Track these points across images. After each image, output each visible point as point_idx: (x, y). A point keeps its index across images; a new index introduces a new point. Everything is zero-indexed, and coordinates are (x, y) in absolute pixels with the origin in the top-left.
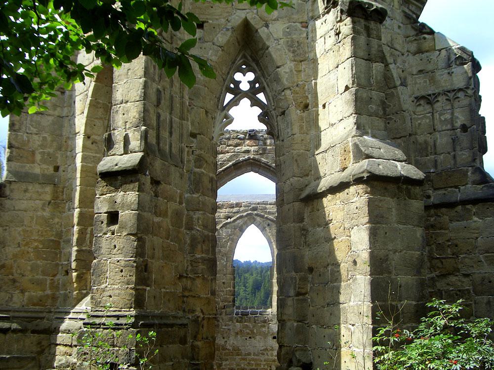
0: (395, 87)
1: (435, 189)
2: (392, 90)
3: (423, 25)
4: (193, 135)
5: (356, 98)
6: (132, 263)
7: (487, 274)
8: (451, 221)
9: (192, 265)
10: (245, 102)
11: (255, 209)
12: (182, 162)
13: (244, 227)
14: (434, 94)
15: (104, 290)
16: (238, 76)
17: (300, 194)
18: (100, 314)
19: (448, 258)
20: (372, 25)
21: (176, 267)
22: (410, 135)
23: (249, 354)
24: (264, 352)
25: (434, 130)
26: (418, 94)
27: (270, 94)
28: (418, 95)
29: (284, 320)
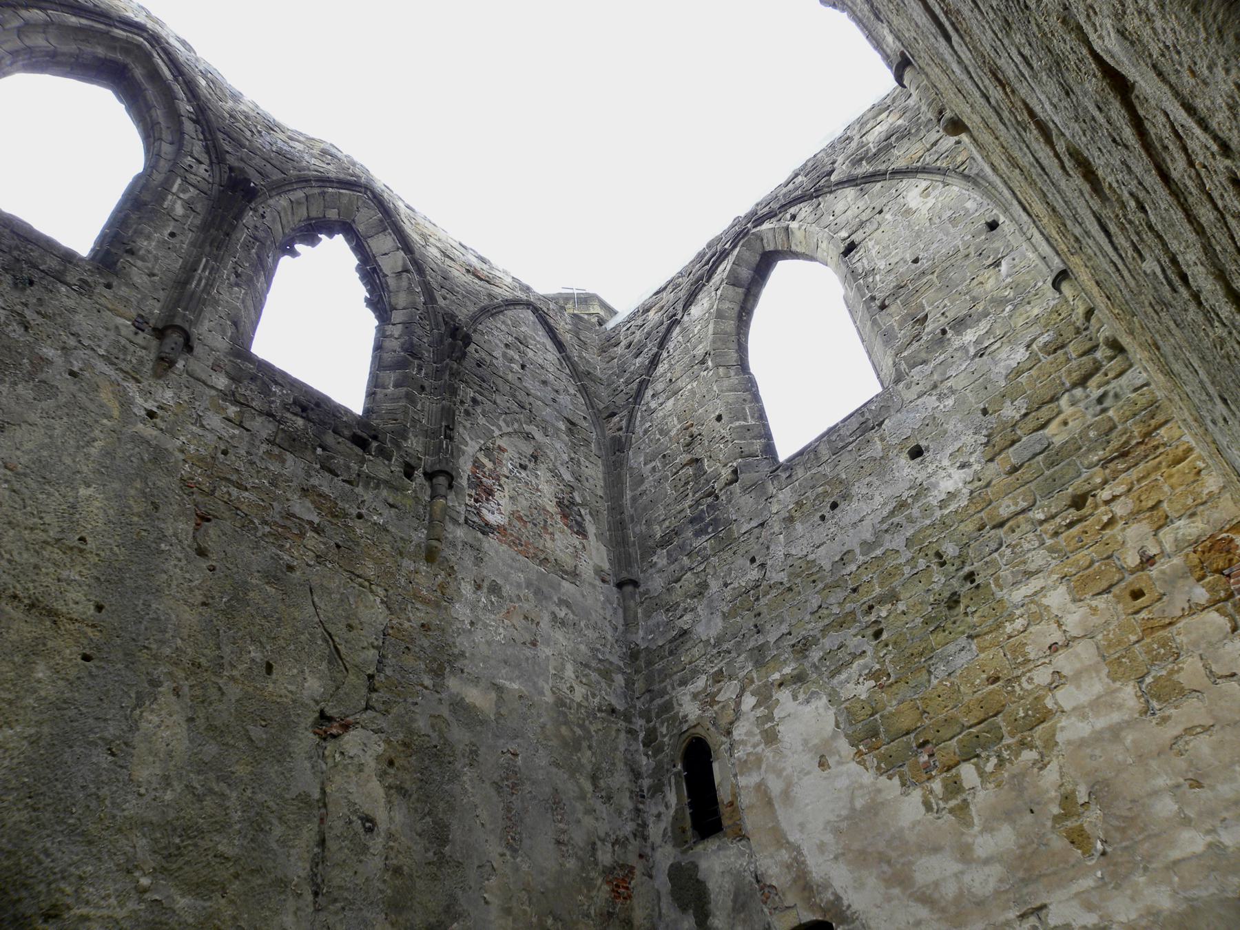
24: (896, 520)
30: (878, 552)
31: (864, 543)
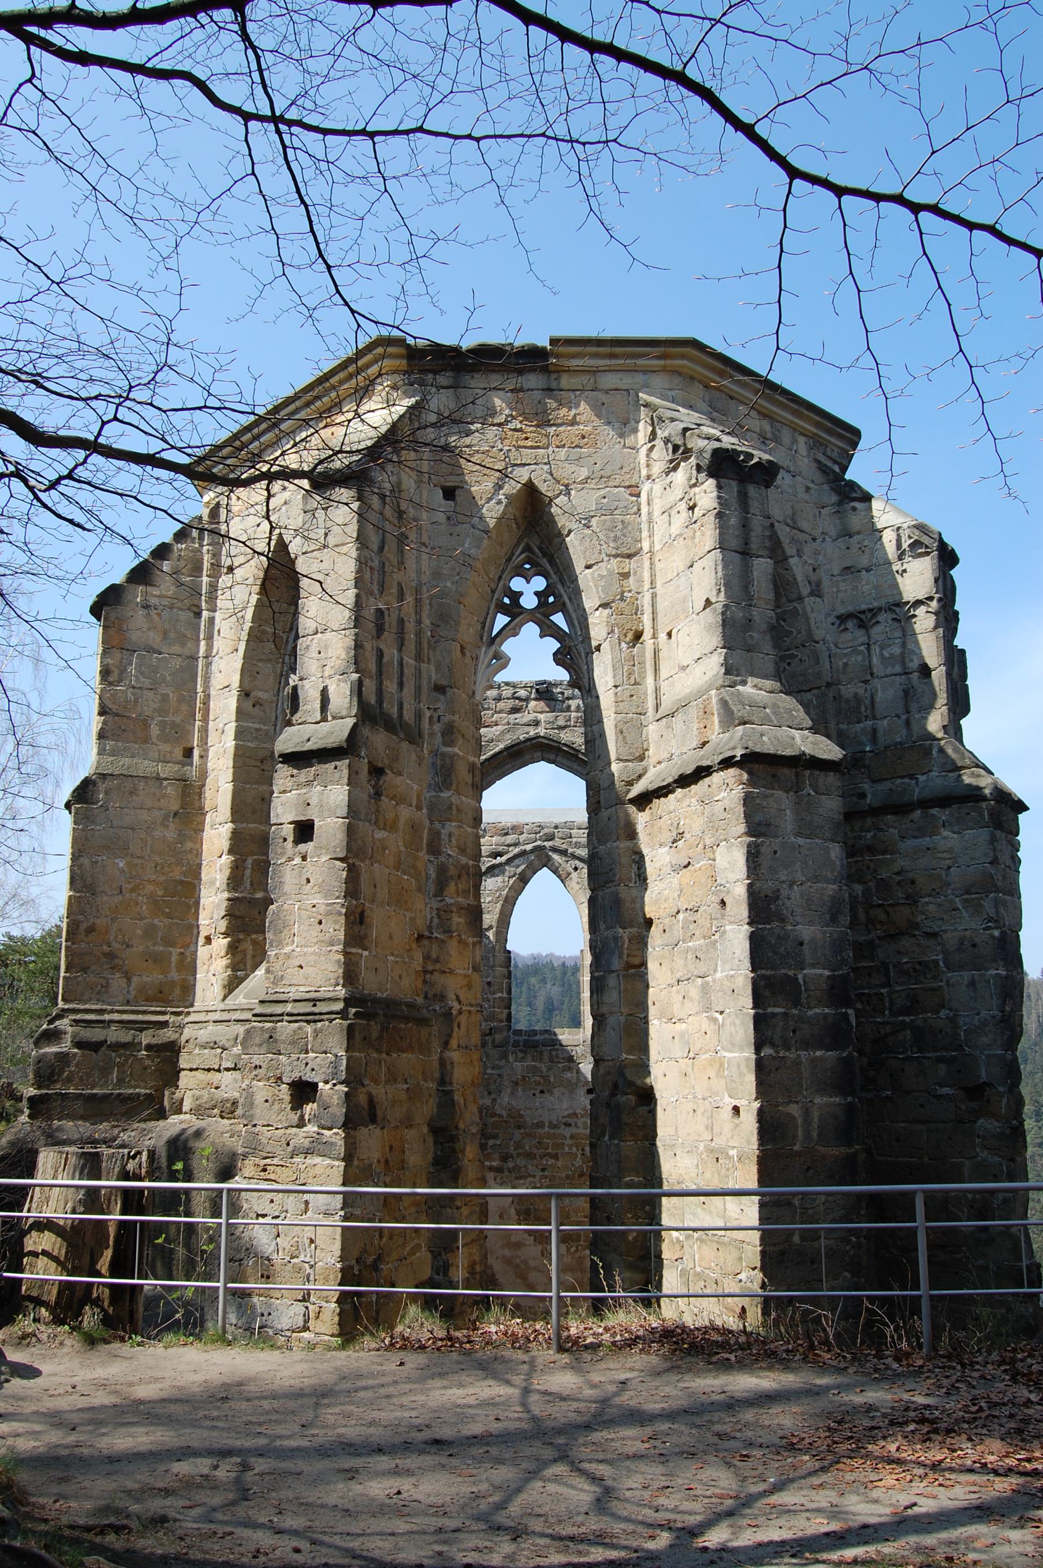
0: (800, 599)
1: (874, 781)
2: (795, 604)
3: (852, 485)
4: (440, 689)
5: (724, 621)
6: (338, 907)
7: (968, 933)
8: (903, 838)
9: (439, 917)
10: (531, 629)
11: (551, 837)
12: (420, 735)
13: (529, 873)
14: (870, 610)
15: (288, 956)
16: (517, 584)
17: (629, 791)
18: (281, 997)
19: (898, 904)
20: (752, 490)
21: (412, 919)
22: (828, 685)
23: (540, 1125)
25: (872, 674)
26: (841, 610)
27: (574, 616)
28: (843, 611)
29: (603, 1015)
30: (556, 1131)
31: (550, 1123)
